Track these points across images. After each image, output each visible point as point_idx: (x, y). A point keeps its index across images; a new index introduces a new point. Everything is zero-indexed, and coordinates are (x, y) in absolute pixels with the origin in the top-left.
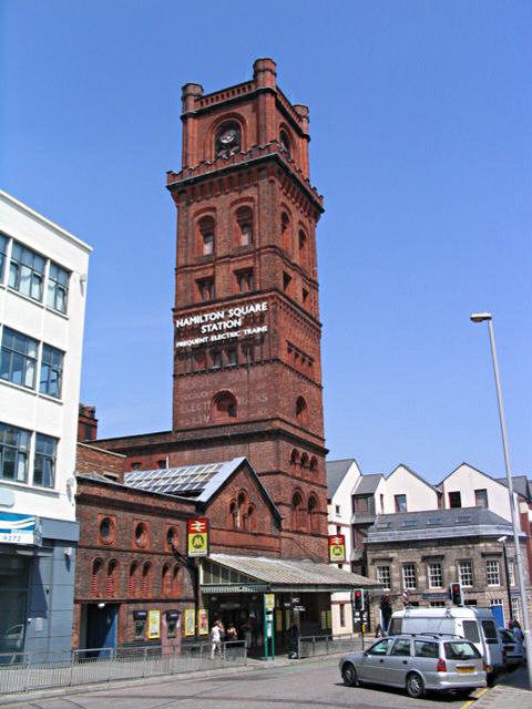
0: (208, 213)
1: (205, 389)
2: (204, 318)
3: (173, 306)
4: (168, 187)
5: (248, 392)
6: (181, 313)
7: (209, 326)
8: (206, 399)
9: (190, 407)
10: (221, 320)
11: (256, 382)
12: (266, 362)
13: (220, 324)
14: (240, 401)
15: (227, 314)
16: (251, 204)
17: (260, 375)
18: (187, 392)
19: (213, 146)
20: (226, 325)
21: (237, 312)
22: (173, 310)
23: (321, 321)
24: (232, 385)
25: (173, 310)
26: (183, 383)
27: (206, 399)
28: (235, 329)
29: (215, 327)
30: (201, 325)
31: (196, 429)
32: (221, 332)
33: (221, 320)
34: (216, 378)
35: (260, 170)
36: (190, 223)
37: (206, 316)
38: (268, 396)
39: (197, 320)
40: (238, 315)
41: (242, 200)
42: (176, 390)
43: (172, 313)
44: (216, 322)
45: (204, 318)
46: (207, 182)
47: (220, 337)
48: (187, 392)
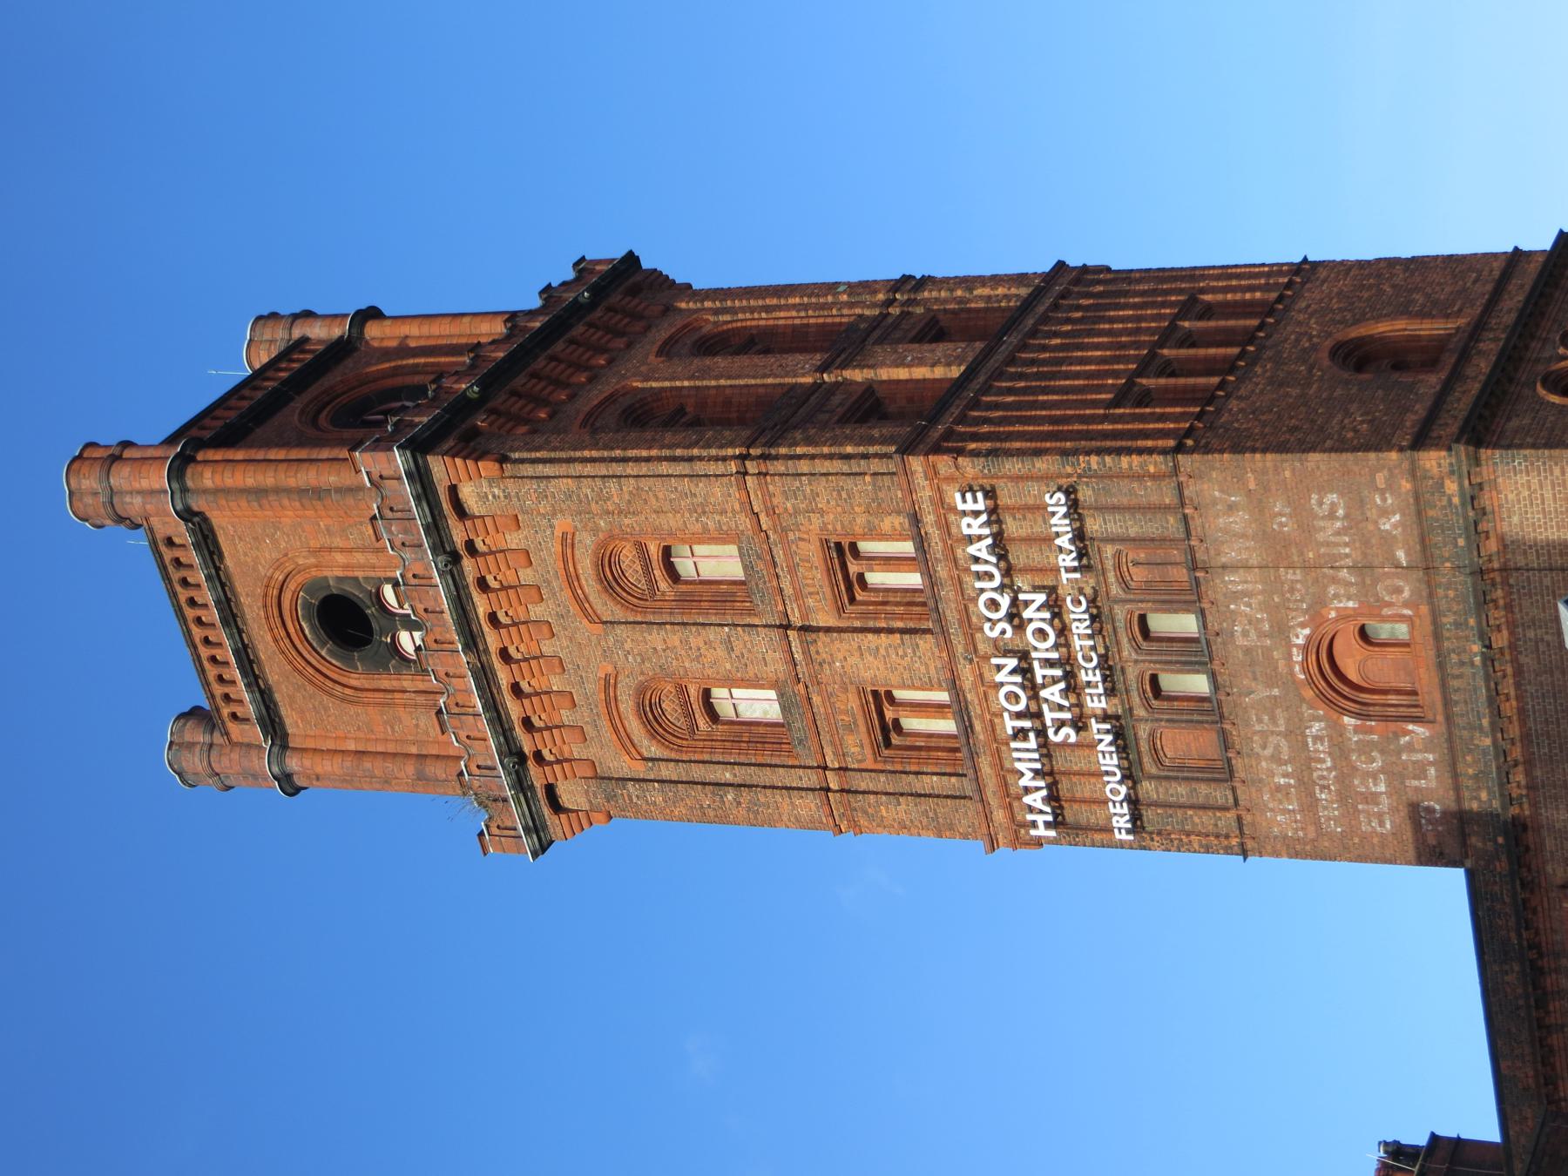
0: (627, 706)
1: (1295, 734)
2: (1021, 734)
3: (980, 845)
4: (543, 847)
5: (1307, 567)
6: (999, 816)
7: (1049, 716)
8: (1337, 732)
9: (1372, 798)
10: (1025, 671)
11: (1267, 537)
13: (1039, 673)
17: (1239, 520)
18: (1310, 805)
19: (385, 683)
20: (1043, 649)
21: (993, 605)
22: (993, 845)
23: (1045, 266)
24: (1281, 631)
25: (993, 845)
26: (1281, 818)
27: (1337, 732)
28: (1055, 607)
29: (1053, 693)
30: (1045, 745)
31: (1455, 776)
33: (1025, 671)
34: (1254, 694)
36: (667, 771)
38: (1322, 491)
39: (1025, 758)
40: (1005, 601)
41: (572, 580)
42: (1297, 849)
43: (1004, 851)
44: (1033, 689)
45: (1021, 734)
47: (1090, 674)
48: (1310, 805)
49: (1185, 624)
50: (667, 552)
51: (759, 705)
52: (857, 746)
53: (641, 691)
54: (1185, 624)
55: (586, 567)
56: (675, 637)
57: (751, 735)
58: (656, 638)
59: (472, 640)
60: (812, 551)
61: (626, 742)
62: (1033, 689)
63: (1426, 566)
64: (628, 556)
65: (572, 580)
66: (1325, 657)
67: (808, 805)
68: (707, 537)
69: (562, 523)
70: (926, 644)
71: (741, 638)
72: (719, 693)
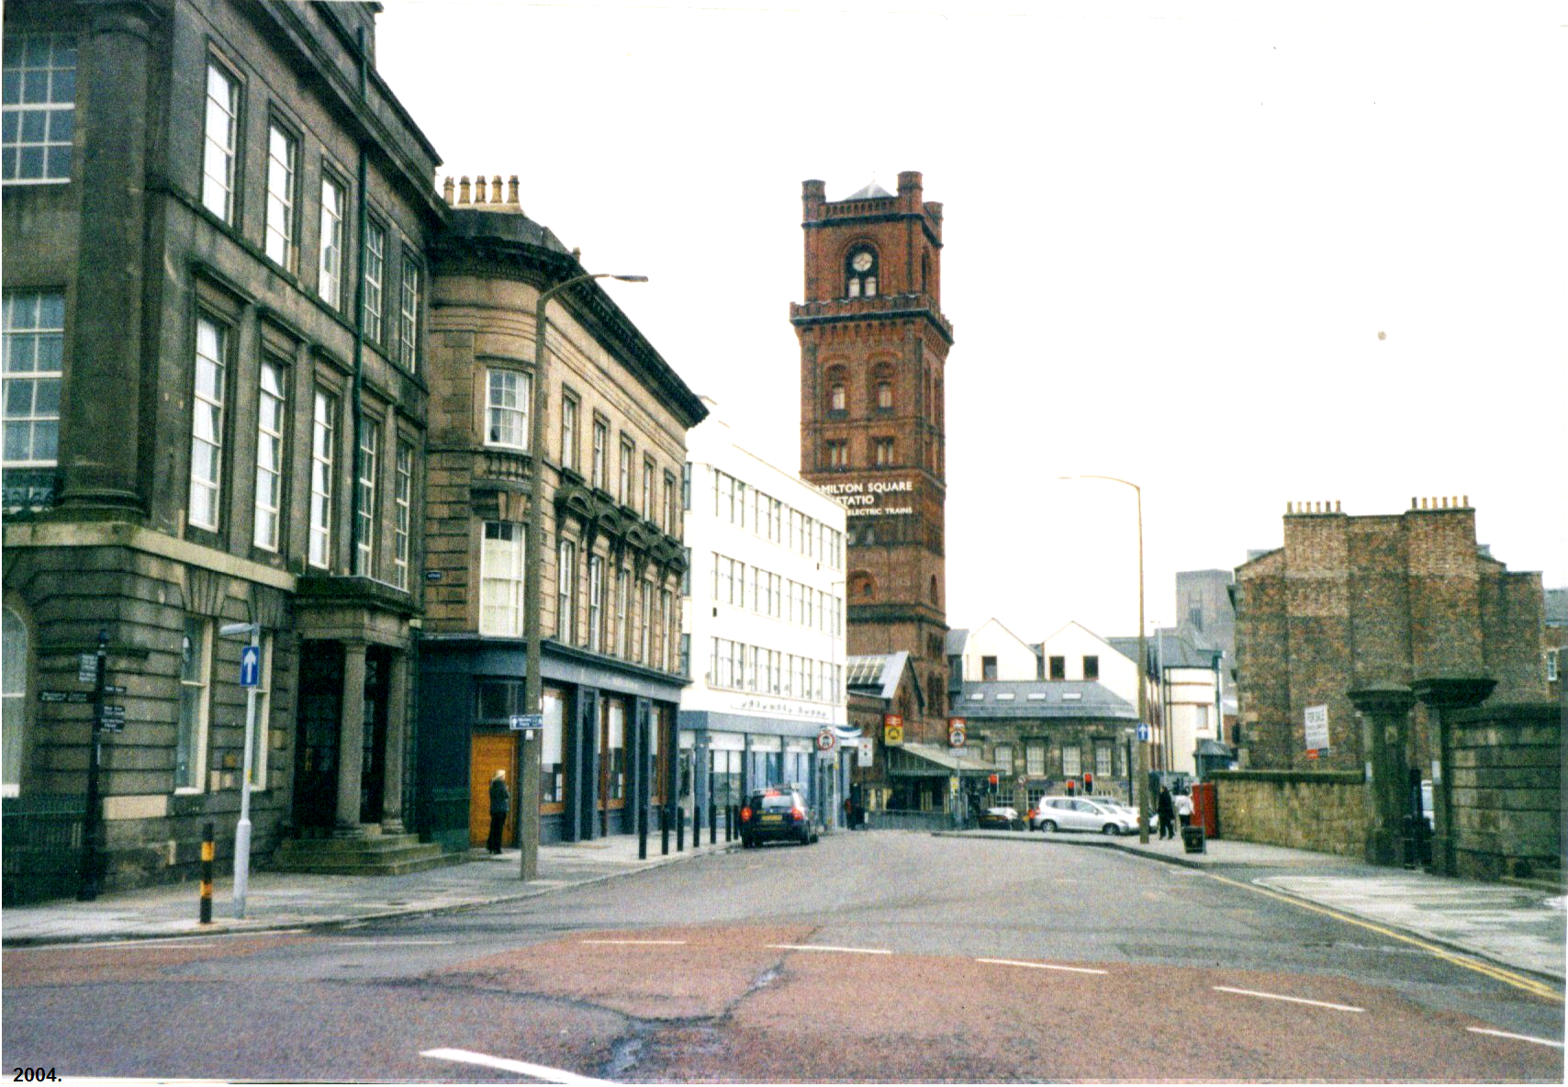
10: (858, 493)
11: (897, 563)
12: (909, 544)
13: (858, 498)
14: (878, 582)
15: (865, 486)
16: (893, 361)
17: (902, 558)
24: (870, 565)
32: (860, 506)
33: (858, 493)
35: (905, 323)
37: (841, 486)
41: (882, 354)
44: (853, 494)
46: (839, 325)
49: (870, 538)
50: (889, 384)
51: (839, 401)
52: (829, 435)
53: (844, 368)
54: (870, 538)
55: (885, 359)
56: (862, 382)
57: (829, 396)
58: (863, 376)
59: (865, 317)
60: (892, 432)
61: (826, 360)
62: (849, 495)
63: (892, 606)
64: (887, 372)
65: (882, 354)
66: (864, 574)
67: (810, 416)
68: (893, 396)
69: (900, 355)
70: (864, 464)
71: (864, 405)
72: (842, 390)
